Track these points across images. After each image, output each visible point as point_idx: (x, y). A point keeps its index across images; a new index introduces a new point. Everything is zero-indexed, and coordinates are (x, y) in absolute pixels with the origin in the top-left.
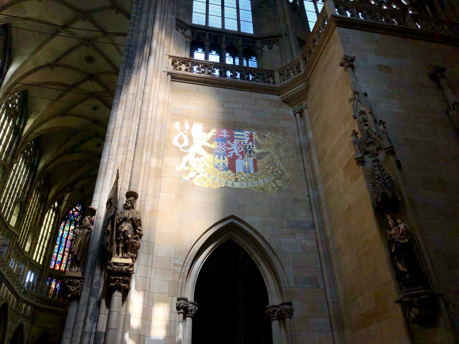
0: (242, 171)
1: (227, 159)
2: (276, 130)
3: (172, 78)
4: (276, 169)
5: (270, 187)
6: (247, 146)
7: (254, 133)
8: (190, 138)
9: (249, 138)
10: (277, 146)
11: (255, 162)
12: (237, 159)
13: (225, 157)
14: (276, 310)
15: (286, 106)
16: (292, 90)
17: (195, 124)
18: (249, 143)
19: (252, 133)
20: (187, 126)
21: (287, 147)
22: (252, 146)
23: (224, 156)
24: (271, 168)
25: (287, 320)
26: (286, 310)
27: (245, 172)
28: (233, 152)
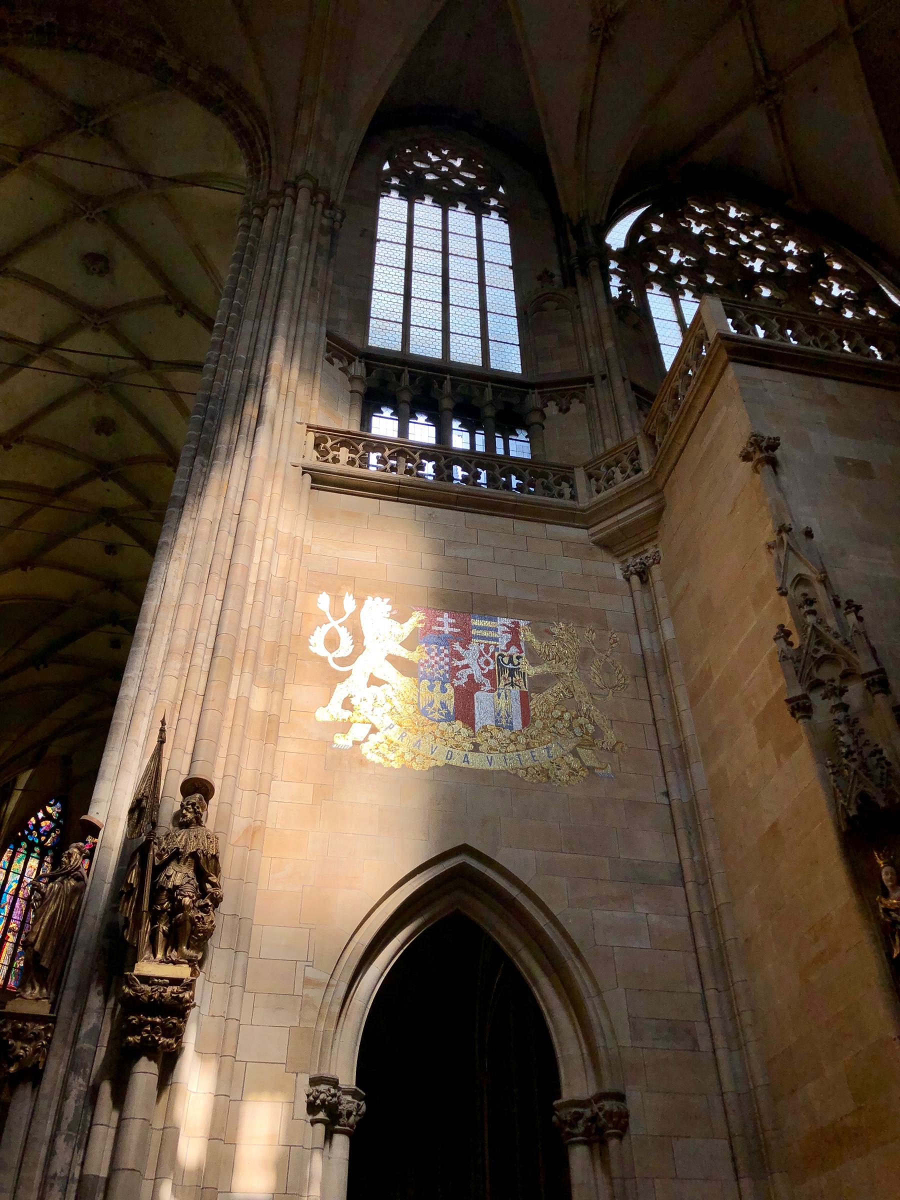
0: (490, 722)
1: (451, 691)
2: (578, 617)
3: (314, 480)
4: (581, 720)
5: (565, 767)
6: (503, 656)
7: (522, 623)
8: (358, 636)
9: (510, 636)
10: (584, 657)
11: (525, 699)
12: (479, 689)
13: (447, 686)
14: (580, 1116)
15: (602, 554)
16: (620, 516)
17: (370, 598)
18: (508, 649)
19: (517, 625)
20: (349, 604)
21: (608, 660)
22: (518, 658)
23: (443, 683)
24: (567, 716)
25: (613, 1143)
26: (610, 1115)
27: (499, 727)
28: (468, 671)
